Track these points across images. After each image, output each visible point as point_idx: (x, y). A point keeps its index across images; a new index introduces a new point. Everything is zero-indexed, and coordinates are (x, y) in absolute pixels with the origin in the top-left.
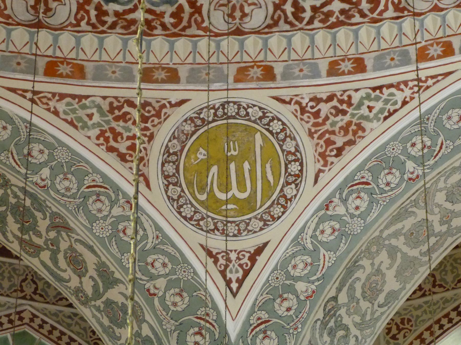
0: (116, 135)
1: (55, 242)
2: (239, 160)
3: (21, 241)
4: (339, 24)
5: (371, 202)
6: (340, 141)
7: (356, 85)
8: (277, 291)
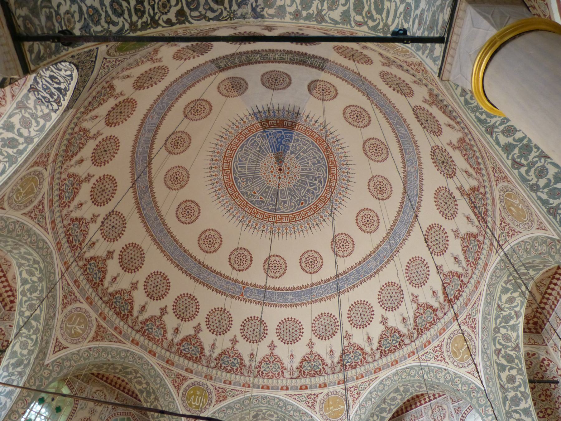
0: (176, 381)
1: (153, 402)
2: (199, 396)
3: (144, 399)
4: (228, 372)
5: (225, 415)
6: (221, 399)
7: (229, 387)
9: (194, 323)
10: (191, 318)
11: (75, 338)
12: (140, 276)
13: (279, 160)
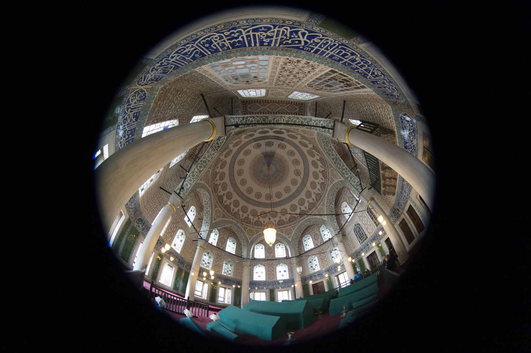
8: (252, 240)
9: (247, 213)
10: (246, 212)
13: (269, 166)
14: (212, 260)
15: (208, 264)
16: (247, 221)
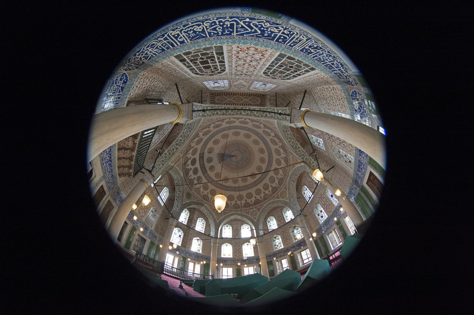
11: (256, 215)
12: (254, 195)
13: (233, 156)
14: (281, 239)
15: (279, 245)
16: (275, 190)
